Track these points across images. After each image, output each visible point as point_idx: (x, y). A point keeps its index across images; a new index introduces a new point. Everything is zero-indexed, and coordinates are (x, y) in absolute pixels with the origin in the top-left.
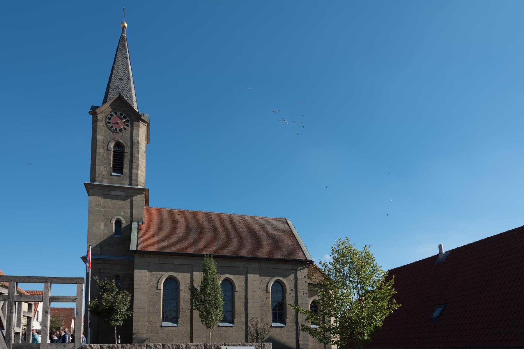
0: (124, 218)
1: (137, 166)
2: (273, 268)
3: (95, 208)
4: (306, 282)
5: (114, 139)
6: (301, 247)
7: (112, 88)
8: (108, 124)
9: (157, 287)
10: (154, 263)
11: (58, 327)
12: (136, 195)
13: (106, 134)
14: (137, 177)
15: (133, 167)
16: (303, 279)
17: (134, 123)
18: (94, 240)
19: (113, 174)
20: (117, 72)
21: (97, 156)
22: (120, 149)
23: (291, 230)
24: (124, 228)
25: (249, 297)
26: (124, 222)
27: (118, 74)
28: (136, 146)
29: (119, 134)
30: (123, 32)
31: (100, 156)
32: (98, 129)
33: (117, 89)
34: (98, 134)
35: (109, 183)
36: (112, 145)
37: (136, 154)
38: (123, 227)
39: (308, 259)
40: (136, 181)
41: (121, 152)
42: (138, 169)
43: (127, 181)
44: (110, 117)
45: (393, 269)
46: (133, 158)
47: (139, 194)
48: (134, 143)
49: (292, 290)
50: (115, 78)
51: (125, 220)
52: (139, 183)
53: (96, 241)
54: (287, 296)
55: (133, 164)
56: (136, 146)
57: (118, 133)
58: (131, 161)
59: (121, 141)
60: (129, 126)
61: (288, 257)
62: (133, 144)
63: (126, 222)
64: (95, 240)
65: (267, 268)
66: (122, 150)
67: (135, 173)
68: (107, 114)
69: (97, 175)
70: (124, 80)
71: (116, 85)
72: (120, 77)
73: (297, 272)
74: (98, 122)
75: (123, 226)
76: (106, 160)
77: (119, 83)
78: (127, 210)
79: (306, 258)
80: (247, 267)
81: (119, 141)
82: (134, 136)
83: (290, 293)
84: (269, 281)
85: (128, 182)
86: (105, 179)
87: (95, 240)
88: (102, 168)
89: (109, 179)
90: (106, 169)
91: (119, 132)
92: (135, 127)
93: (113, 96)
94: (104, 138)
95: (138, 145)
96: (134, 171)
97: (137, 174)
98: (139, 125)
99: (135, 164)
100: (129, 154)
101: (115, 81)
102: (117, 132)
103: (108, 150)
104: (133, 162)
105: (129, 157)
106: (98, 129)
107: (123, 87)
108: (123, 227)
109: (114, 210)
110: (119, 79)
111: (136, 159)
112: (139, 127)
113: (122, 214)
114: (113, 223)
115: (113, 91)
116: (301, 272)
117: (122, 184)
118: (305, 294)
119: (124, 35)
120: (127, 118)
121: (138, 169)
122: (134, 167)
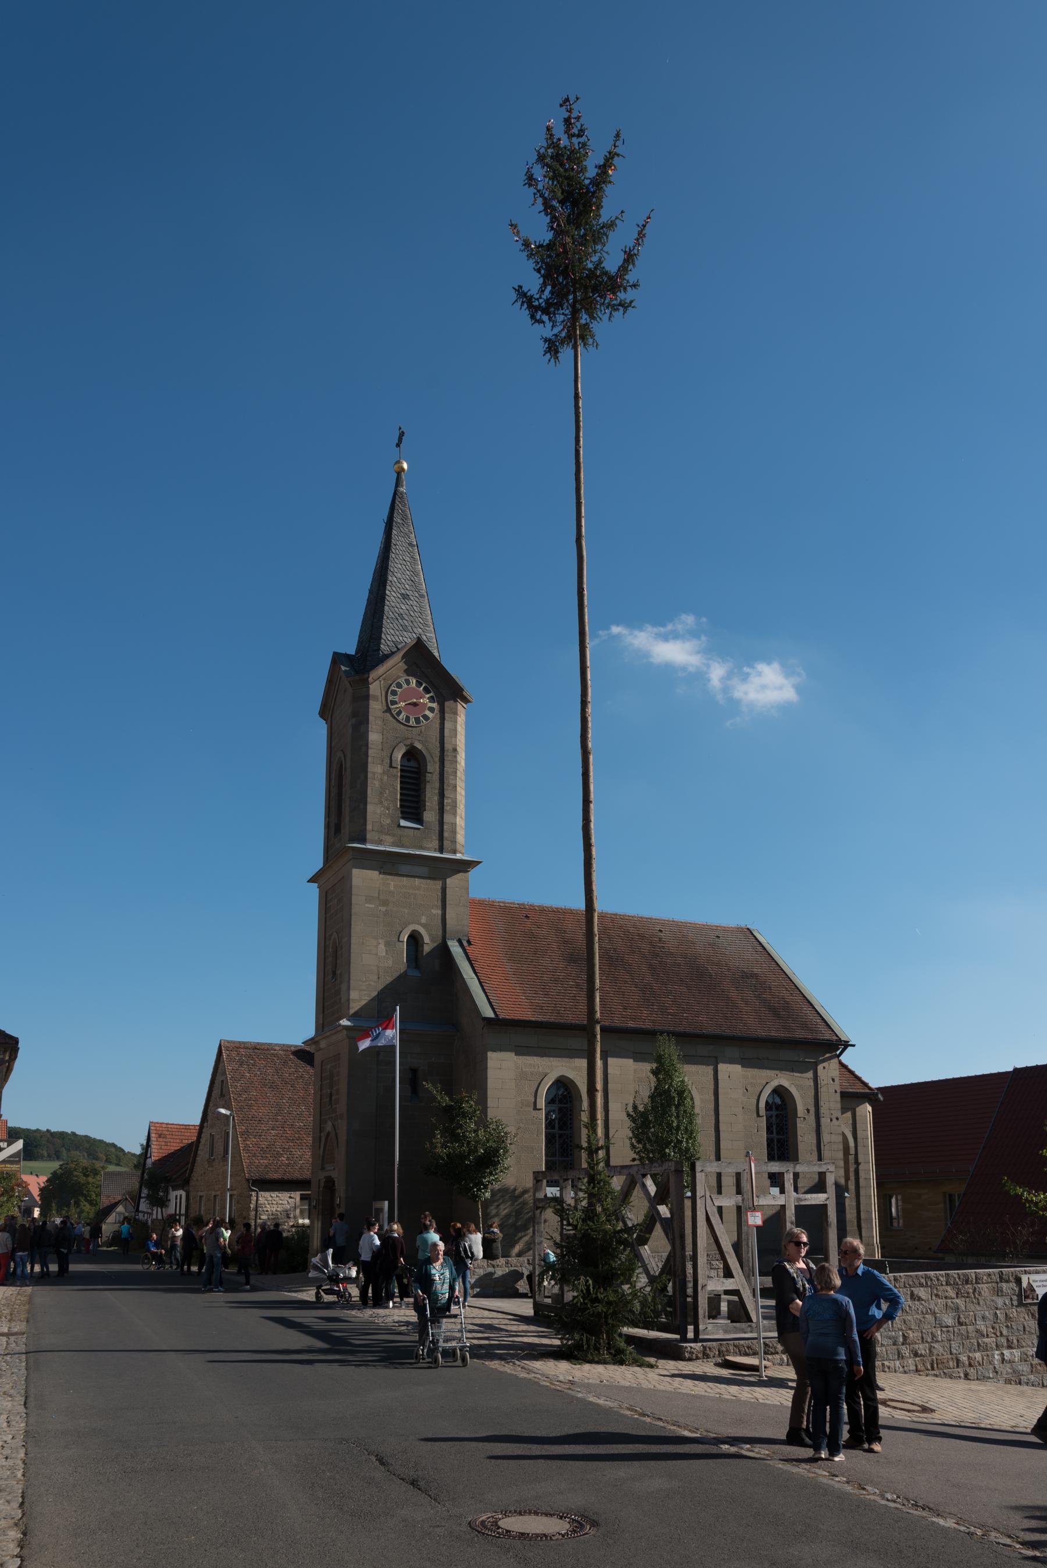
0: (427, 930)
1: (454, 806)
2: (768, 1059)
3: (367, 905)
4: (836, 1092)
5: (405, 742)
6: (814, 1008)
7: (388, 617)
8: (392, 705)
9: (535, 1103)
10: (527, 1047)
11: (714, 1317)
12: (454, 875)
13: (386, 730)
14: (454, 832)
15: (445, 808)
16: (831, 1084)
17: (447, 704)
18: (364, 982)
19: (403, 823)
20: (395, 579)
21: (369, 781)
23: (773, 959)
24: (428, 954)
25: (722, 1127)
26: (427, 939)
27: (398, 584)
28: (450, 758)
29: (414, 729)
30: (398, 483)
31: (375, 782)
32: (370, 717)
33: (400, 621)
34: (370, 730)
35: (394, 845)
36: (398, 755)
37: (452, 777)
38: (424, 954)
39: (842, 1039)
40: (452, 842)
41: (413, 770)
42: (455, 814)
43: (432, 841)
44: (396, 689)
45: (1027, 1068)
46: (445, 788)
47: (459, 872)
48: (448, 751)
49: (808, 1111)
50: (393, 593)
51: (430, 935)
52: (458, 847)
53: (370, 985)
54: (798, 1125)
55: (445, 801)
56: (450, 758)
57: (411, 727)
58: (442, 795)
59: (418, 746)
60: (436, 711)
61: (800, 1034)
62: (445, 753)
63: (432, 940)
64: (367, 983)
65: (758, 1058)
66: (417, 766)
67: (448, 823)
68: (390, 682)
69: (369, 827)
70: (412, 599)
71: (396, 609)
72: (403, 591)
73: (817, 1069)
74: (371, 702)
75: (427, 949)
76: (387, 792)
77: (402, 605)
78: (433, 911)
79: (837, 1036)
80: (715, 1057)
81: (415, 745)
82: (446, 735)
83: (804, 1118)
84: (761, 1092)
85: (435, 844)
86: (386, 837)
87: (367, 983)
88: (379, 810)
89: (394, 836)
90: (387, 812)
93: (392, 637)
94: (383, 739)
95: (456, 757)
96: (447, 818)
97: (454, 825)
98: (456, 709)
99: (450, 801)
100: (435, 777)
101: (394, 600)
103: (391, 766)
104: (444, 795)
105: (437, 785)
106: (371, 718)
107: (412, 614)
108: (424, 954)
109: (406, 911)
110: (402, 594)
111: (450, 788)
112: (455, 713)
113: (423, 920)
114: (403, 941)
115: (391, 625)
116: (824, 1068)
117: (422, 848)
118: (834, 1120)
119: (401, 489)
120: (430, 692)
121: (456, 812)
122: (447, 808)
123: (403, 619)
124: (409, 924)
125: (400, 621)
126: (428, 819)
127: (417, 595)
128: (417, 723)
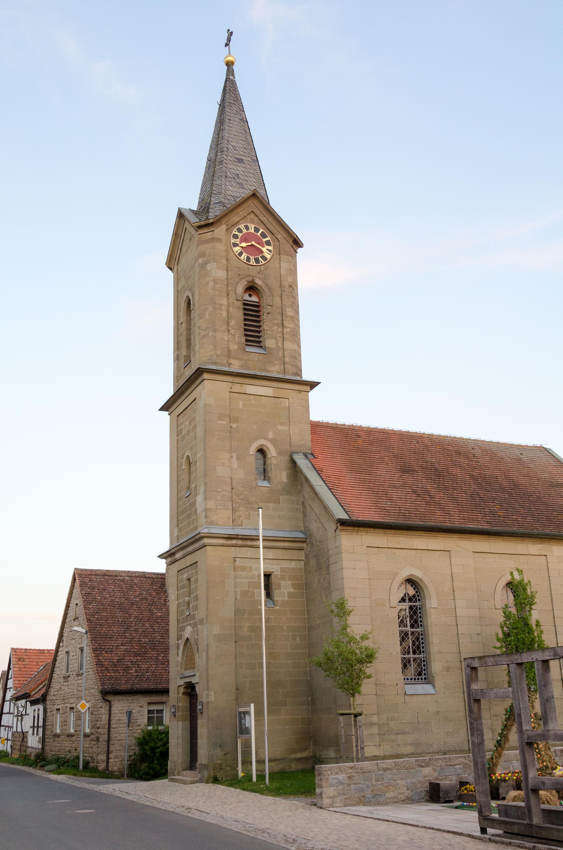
0: (274, 445)
3: (219, 422)
22: (254, 298)
44: (237, 233)
57: (252, 265)
59: (259, 282)
66: (258, 301)
78: (278, 427)
81: (255, 281)
89: (241, 359)
91: (255, 264)
92: (283, 255)
102: (251, 263)
113: (271, 435)
120: (267, 237)
123: (239, 178)
124: (257, 439)
125: (237, 180)
126: (270, 346)
127: (250, 160)
128: (256, 263)
